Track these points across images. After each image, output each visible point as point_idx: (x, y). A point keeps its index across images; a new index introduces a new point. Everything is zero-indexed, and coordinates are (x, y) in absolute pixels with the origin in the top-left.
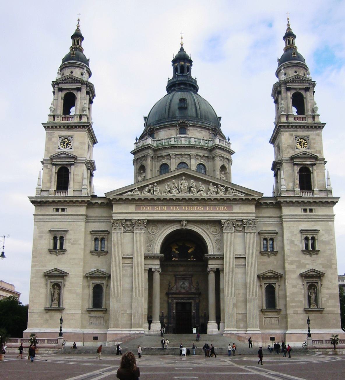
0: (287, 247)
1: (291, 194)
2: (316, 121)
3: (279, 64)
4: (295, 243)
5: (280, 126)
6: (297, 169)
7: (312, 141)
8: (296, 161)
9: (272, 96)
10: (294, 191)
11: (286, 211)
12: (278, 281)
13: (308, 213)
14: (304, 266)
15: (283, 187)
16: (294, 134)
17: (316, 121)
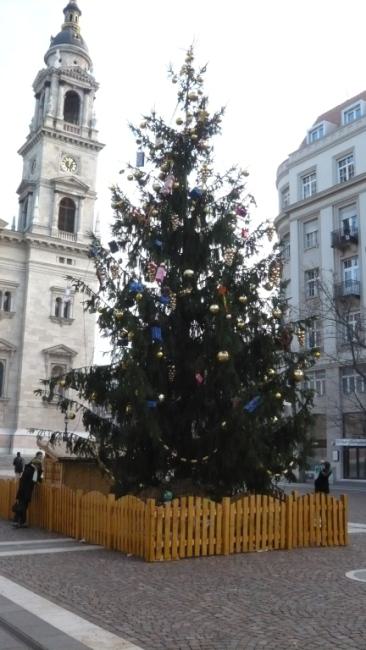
0: (29, 309)
1: (45, 232)
2: (93, 137)
3: (52, 45)
4: (43, 303)
5: (44, 132)
6: (58, 198)
7: (83, 165)
8: (58, 187)
9: (34, 86)
10: (50, 228)
11: (35, 255)
12: (10, 357)
13: (65, 264)
14: (51, 338)
15: (36, 221)
16: (61, 148)
17: (93, 137)
